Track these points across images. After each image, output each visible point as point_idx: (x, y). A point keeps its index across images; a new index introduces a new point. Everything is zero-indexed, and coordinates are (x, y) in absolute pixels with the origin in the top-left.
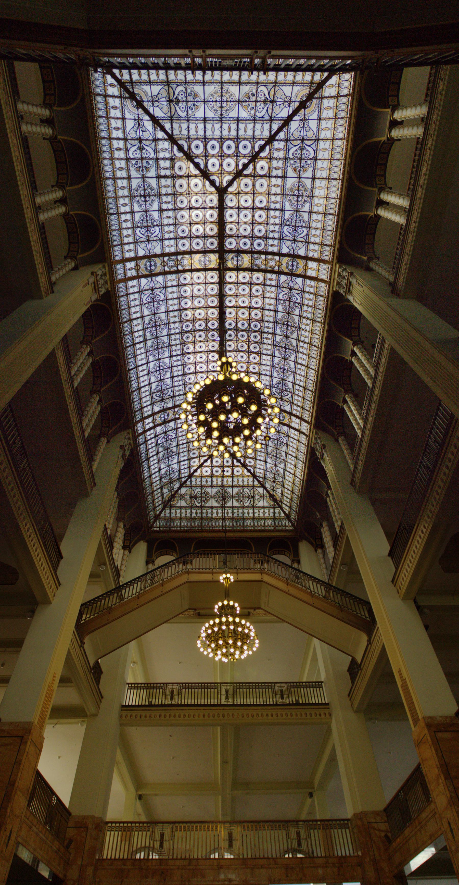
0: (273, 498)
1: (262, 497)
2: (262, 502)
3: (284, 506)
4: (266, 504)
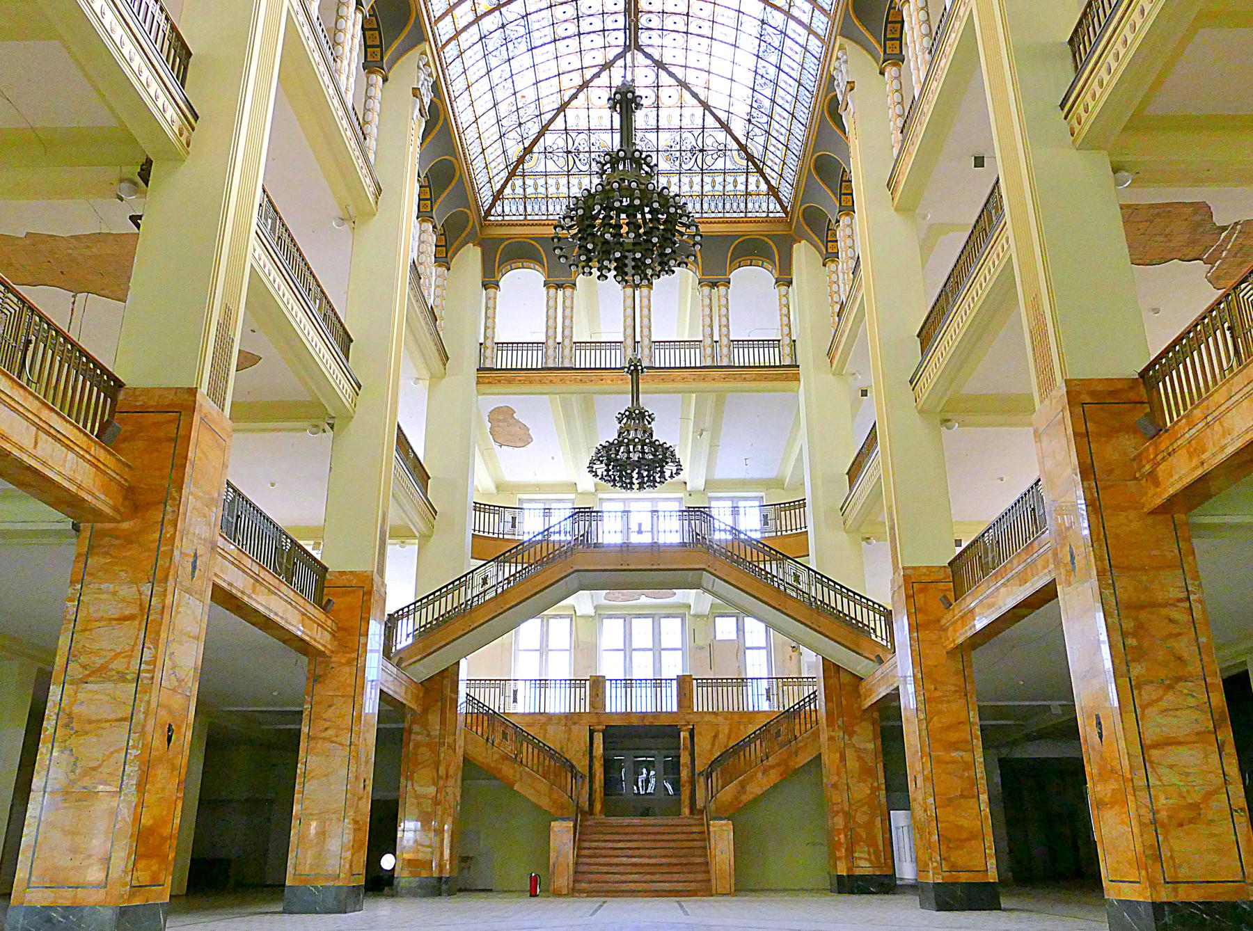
0: (746, 152)
1: (723, 151)
2: (721, 160)
3: (767, 170)
4: (729, 166)
